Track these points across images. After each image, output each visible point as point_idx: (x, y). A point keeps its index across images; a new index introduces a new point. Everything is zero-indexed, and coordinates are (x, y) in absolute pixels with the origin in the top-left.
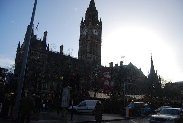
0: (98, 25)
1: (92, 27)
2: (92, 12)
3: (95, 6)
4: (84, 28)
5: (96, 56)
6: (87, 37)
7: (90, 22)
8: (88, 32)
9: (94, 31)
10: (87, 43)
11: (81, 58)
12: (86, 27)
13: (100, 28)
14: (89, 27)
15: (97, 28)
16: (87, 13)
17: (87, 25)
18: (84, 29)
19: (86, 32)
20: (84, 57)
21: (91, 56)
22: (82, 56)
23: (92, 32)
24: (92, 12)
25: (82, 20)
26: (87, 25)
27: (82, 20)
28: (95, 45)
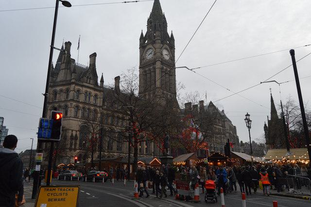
1: (162, 45)
2: (157, 20)
4: (148, 47)
5: (169, 94)
6: (154, 62)
8: (155, 54)
9: (165, 52)
10: (155, 72)
11: (145, 95)
12: (151, 46)
14: (158, 45)
15: (167, 47)
16: (149, 22)
17: (154, 43)
18: (146, 49)
23: (162, 54)
24: (157, 20)
25: (142, 33)
27: (142, 33)
28: (167, 76)
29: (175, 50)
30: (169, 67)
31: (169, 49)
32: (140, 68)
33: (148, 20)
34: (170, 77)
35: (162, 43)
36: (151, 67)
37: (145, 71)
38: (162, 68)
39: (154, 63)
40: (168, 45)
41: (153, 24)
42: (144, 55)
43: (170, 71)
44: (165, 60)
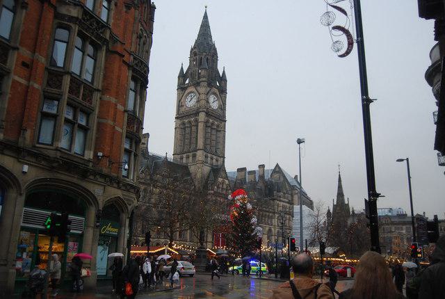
1: (209, 89)
5: (215, 157)
7: (204, 79)
8: (198, 102)
9: (212, 98)
10: (197, 126)
11: (182, 158)
12: (192, 89)
13: (223, 91)
14: (202, 90)
15: (216, 91)
16: (194, 53)
17: (197, 84)
18: (187, 92)
19: (194, 100)
20: (188, 157)
21: (206, 157)
22: (185, 156)
23: (208, 102)
25: (182, 68)
26: (197, 84)
27: (182, 68)
28: (214, 132)
30: (217, 120)
31: (218, 93)
33: (192, 49)
35: (210, 85)
36: (192, 119)
37: (184, 124)
38: (207, 122)
39: (197, 114)
40: (217, 88)
42: (182, 100)
43: (218, 126)
44: (213, 110)
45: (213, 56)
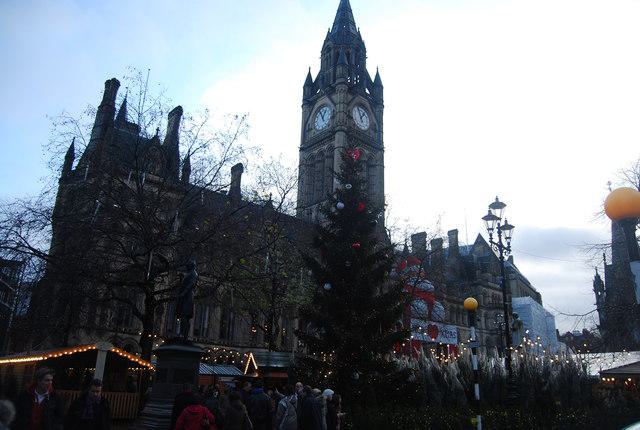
0: (367, 91)
1: (350, 97)
3: (354, 24)
4: (320, 103)
6: (330, 134)
8: (333, 117)
9: (356, 114)
12: (325, 100)
14: (337, 97)
16: (326, 50)
18: (317, 106)
19: (327, 116)
23: (350, 117)
25: (309, 74)
27: (309, 74)
29: (385, 110)
31: (368, 104)
32: (301, 149)
34: (372, 169)
35: (352, 90)
37: (312, 157)
41: (332, 52)
43: (370, 158)
44: (359, 131)
45: (357, 50)
